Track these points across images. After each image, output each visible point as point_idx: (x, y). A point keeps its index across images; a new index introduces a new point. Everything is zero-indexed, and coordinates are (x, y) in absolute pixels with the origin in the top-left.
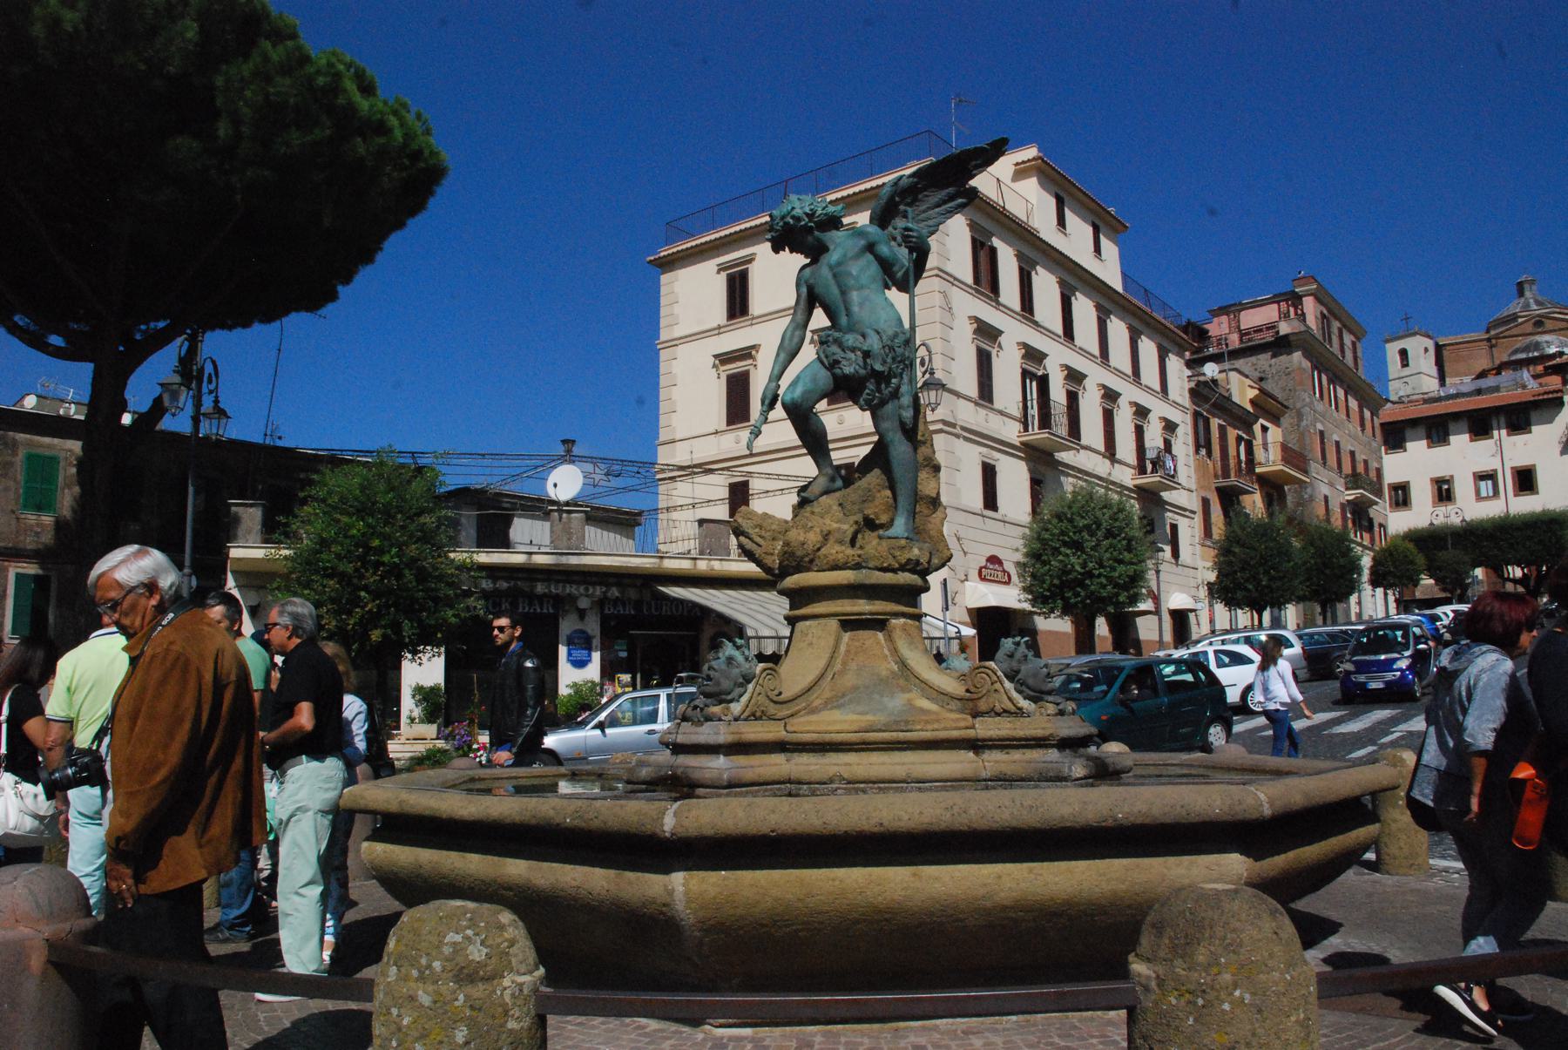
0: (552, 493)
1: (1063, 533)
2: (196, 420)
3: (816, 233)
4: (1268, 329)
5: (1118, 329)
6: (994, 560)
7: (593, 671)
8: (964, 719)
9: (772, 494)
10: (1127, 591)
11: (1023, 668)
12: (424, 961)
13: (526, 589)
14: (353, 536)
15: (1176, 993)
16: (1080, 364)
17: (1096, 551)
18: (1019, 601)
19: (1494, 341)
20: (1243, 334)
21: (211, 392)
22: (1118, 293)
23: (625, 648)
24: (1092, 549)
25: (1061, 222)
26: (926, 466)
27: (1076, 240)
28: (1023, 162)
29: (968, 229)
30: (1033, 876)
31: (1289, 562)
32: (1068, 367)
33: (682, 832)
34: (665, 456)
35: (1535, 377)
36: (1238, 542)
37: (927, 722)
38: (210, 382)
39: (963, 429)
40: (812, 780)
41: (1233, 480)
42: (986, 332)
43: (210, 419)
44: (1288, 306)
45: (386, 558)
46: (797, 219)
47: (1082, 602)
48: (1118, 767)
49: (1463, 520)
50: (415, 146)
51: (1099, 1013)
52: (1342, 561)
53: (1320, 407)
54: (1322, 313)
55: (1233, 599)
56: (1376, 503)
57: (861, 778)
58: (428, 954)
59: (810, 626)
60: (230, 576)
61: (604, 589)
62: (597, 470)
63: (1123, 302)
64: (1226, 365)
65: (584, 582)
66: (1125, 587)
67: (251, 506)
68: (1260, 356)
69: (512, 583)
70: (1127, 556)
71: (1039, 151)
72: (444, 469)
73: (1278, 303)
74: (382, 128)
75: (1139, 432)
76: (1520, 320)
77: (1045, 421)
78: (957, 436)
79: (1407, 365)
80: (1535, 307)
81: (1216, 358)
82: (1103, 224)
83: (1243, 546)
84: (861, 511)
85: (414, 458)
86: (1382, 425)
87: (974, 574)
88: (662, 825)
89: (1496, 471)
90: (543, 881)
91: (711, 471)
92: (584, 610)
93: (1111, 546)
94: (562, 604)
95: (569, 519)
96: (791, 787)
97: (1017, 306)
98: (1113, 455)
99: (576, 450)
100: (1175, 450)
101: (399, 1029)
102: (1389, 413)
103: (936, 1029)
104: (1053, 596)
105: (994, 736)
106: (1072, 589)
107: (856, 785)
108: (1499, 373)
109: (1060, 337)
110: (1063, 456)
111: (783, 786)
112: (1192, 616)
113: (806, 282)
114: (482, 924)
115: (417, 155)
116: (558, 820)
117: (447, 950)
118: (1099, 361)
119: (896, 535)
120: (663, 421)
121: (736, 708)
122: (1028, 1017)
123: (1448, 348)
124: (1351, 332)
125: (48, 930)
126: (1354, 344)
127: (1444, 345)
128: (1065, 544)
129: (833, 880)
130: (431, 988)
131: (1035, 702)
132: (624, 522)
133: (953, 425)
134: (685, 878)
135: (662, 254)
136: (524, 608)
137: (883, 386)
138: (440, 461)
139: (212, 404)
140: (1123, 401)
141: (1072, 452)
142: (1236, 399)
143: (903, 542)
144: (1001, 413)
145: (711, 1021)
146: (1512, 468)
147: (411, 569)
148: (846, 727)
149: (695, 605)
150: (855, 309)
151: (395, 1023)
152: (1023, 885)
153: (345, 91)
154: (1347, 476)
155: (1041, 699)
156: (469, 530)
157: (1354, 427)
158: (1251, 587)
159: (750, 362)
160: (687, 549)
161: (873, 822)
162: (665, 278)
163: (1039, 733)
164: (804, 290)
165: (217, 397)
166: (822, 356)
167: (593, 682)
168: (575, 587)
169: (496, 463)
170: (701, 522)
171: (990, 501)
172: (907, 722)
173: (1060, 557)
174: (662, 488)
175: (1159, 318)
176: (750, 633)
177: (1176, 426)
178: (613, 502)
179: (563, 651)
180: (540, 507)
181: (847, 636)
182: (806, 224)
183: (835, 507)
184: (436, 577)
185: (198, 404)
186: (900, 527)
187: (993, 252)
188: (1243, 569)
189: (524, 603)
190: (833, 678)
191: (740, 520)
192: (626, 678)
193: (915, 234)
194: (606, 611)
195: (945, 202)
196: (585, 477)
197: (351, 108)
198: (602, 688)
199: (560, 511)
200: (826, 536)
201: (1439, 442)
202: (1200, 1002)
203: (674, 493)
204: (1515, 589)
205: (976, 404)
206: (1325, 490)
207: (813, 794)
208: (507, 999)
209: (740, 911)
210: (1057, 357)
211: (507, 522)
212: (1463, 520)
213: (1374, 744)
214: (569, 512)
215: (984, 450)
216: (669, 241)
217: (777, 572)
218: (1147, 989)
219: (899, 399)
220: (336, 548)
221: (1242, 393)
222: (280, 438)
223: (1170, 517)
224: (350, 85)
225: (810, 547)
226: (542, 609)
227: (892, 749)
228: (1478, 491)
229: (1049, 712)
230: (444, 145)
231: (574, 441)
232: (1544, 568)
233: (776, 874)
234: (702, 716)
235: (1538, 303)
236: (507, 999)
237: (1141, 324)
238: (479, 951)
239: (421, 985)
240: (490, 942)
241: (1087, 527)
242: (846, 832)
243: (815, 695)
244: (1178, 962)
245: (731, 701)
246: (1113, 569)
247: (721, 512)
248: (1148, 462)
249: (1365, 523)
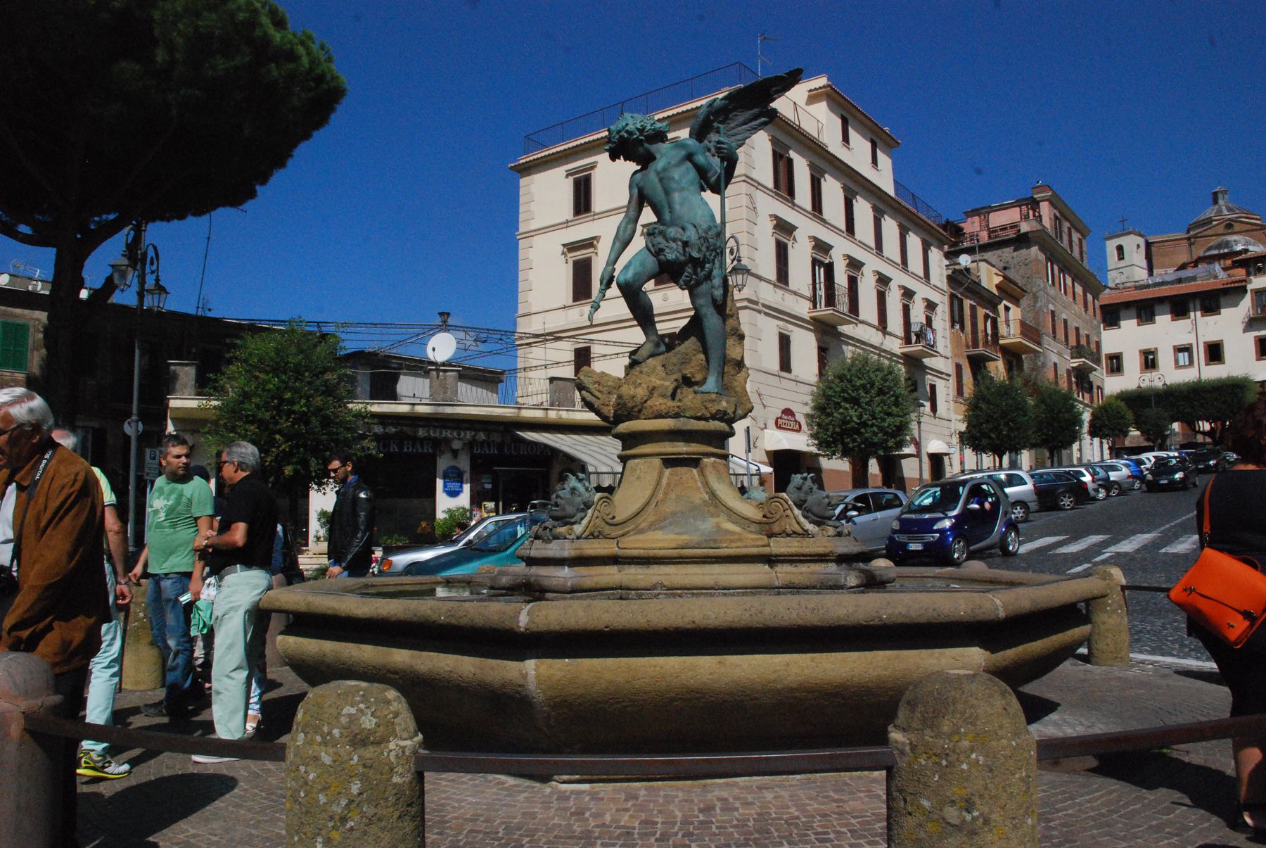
0: (431, 356)
1: (843, 391)
2: (141, 295)
3: (646, 145)
4: (1012, 227)
5: (890, 226)
6: (788, 412)
7: (464, 500)
8: (761, 539)
9: (609, 357)
10: (895, 438)
11: (809, 498)
12: (325, 729)
13: (410, 433)
14: (269, 390)
15: (925, 755)
16: (859, 254)
17: (870, 405)
18: (808, 445)
19: (1192, 240)
20: (991, 232)
21: (153, 272)
22: (889, 196)
23: (490, 481)
24: (866, 404)
25: (846, 138)
26: (733, 335)
27: (858, 153)
28: (816, 89)
29: (769, 143)
30: (814, 664)
31: (1025, 416)
32: (849, 257)
33: (534, 628)
34: (526, 326)
35: (1225, 269)
36: (984, 400)
37: (732, 541)
38: (152, 263)
39: (764, 306)
40: (639, 587)
41: (981, 349)
42: (784, 228)
43: (153, 294)
44: (1028, 209)
45: (296, 408)
46: (630, 133)
47: (858, 446)
48: (885, 578)
49: (1165, 384)
50: (318, 71)
51: (866, 773)
52: (1067, 416)
53: (1052, 291)
54: (1055, 214)
55: (979, 445)
56: (1095, 370)
57: (679, 586)
58: (328, 724)
59: (638, 463)
60: (169, 422)
61: (473, 433)
62: (468, 337)
63: (893, 203)
64: (977, 257)
65: (454, 428)
66: (893, 435)
67: (187, 365)
68: (1004, 250)
69: (399, 428)
71: (828, 80)
72: (343, 336)
73: (1020, 206)
74: (292, 56)
75: (906, 310)
76: (1214, 223)
77: (830, 301)
78: (760, 312)
79: (1123, 258)
80: (1227, 213)
81: (970, 251)
82: (879, 140)
83: (988, 402)
84: (680, 371)
85: (319, 326)
86: (1101, 307)
87: (771, 423)
88: (518, 622)
89: (1191, 345)
90: (422, 667)
91: (560, 339)
92: (458, 450)
93: (882, 401)
94: (440, 445)
95: (445, 379)
96: (622, 592)
97: (809, 207)
98: (885, 328)
99: (451, 321)
100: (934, 325)
101: (306, 783)
102: (1107, 297)
103: (736, 784)
104: (835, 441)
105: (786, 553)
107: (673, 591)
108: (1196, 266)
109: (843, 232)
110: (844, 329)
111: (615, 592)
112: (946, 459)
113: (637, 185)
114: (373, 700)
115: (320, 79)
116: (434, 617)
117: (344, 720)
118: (874, 252)
119: (708, 390)
120: (521, 297)
121: (578, 529)
122: (809, 776)
123: (1156, 245)
124: (1078, 231)
125: (24, 705)
126: (1080, 240)
127: (1154, 243)
128: (845, 400)
129: (655, 666)
130: (331, 750)
131: (818, 526)
132: (489, 379)
133: (756, 303)
134: (536, 664)
135: (521, 162)
136: (408, 449)
137: (699, 269)
138: (341, 329)
139: (154, 282)
140: (893, 285)
141: (851, 326)
142: (984, 284)
143: (714, 396)
144: (795, 293)
145: (556, 777)
146: (1205, 343)
147: (317, 417)
148: (666, 545)
149: (546, 446)
150: (677, 207)
151: (303, 778)
152: (806, 671)
153: (261, 25)
154: (1072, 348)
155: (824, 524)
156: (364, 385)
157: (1079, 308)
158: (994, 436)
159: (592, 250)
160: (540, 401)
161: (686, 620)
162: (523, 181)
163: (821, 550)
164: (636, 191)
165: (158, 276)
166: (650, 245)
167: (464, 508)
168: (449, 431)
169: (384, 331)
170: (552, 380)
171: (785, 365)
172: (715, 541)
173: (841, 410)
174: (520, 352)
175: (924, 218)
176: (591, 469)
177: (937, 305)
178: (480, 363)
179: (440, 483)
180: (421, 367)
181: (668, 472)
182: (637, 138)
183: (660, 368)
184: (337, 423)
185: (142, 282)
186: (711, 384)
187: (790, 162)
188: (988, 421)
189: (408, 443)
190: (656, 506)
191: (582, 378)
192: (491, 505)
193: (723, 146)
194: (475, 451)
195: (751, 120)
196: (458, 343)
197: (266, 40)
198: (471, 513)
199: (438, 370)
200: (652, 391)
201: (1147, 320)
202: (944, 763)
203: (530, 356)
204: (1204, 439)
205: (775, 285)
206: (1054, 358)
207: (640, 597)
208: (393, 759)
209: (580, 691)
210: (841, 249)
211: (394, 379)
212: (1165, 384)
213: (1089, 562)
214: (445, 371)
215: (781, 323)
216: (526, 152)
217: (612, 419)
218: (902, 753)
219: (711, 280)
220: (256, 400)
221: (990, 280)
222: (210, 310)
223: (929, 379)
224: (265, 20)
225: (638, 399)
226: (422, 448)
227: (705, 563)
228: (1176, 361)
229: (829, 534)
230: (342, 71)
231: (448, 314)
232: (1228, 423)
233: (610, 662)
234: (552, 535)
235: (1229, 209)
236: (393, 759)
237: (909, 222)
238: (370, 721)
239: (324, 748)
240: (378, 714)
241: (863, 386)
242: (665, 628)
243: (642, 519)
244: (928, 731)
245: (574, 523)
246: (883, 420)
247: (568, 372)
248: (913, 335)
249: (1086, 385)
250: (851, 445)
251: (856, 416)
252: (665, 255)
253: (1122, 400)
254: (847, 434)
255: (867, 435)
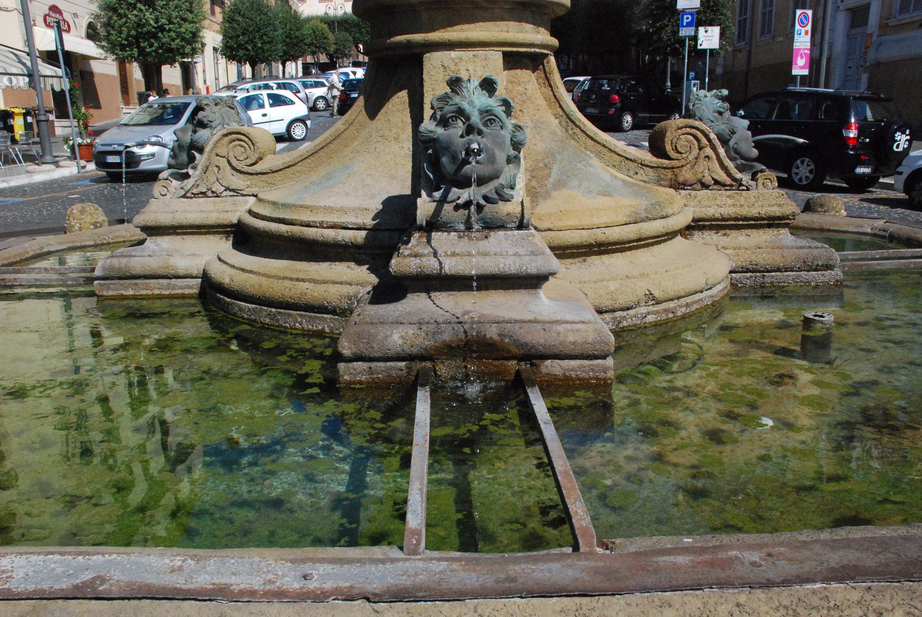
10: (190, 45)
17: (166, 9)
36: (239, 13)
47: (156, 51)
66: (189, 42)
70: (190, 16)
83: (243, 16)
104: (130, 45)
106: (147, 40)
173: (135, 12)
188: (244, 34)
250: (148, 50)
251: (153, 20)
253: (325, 23)
254: (142, 38)
255: (164, 40)
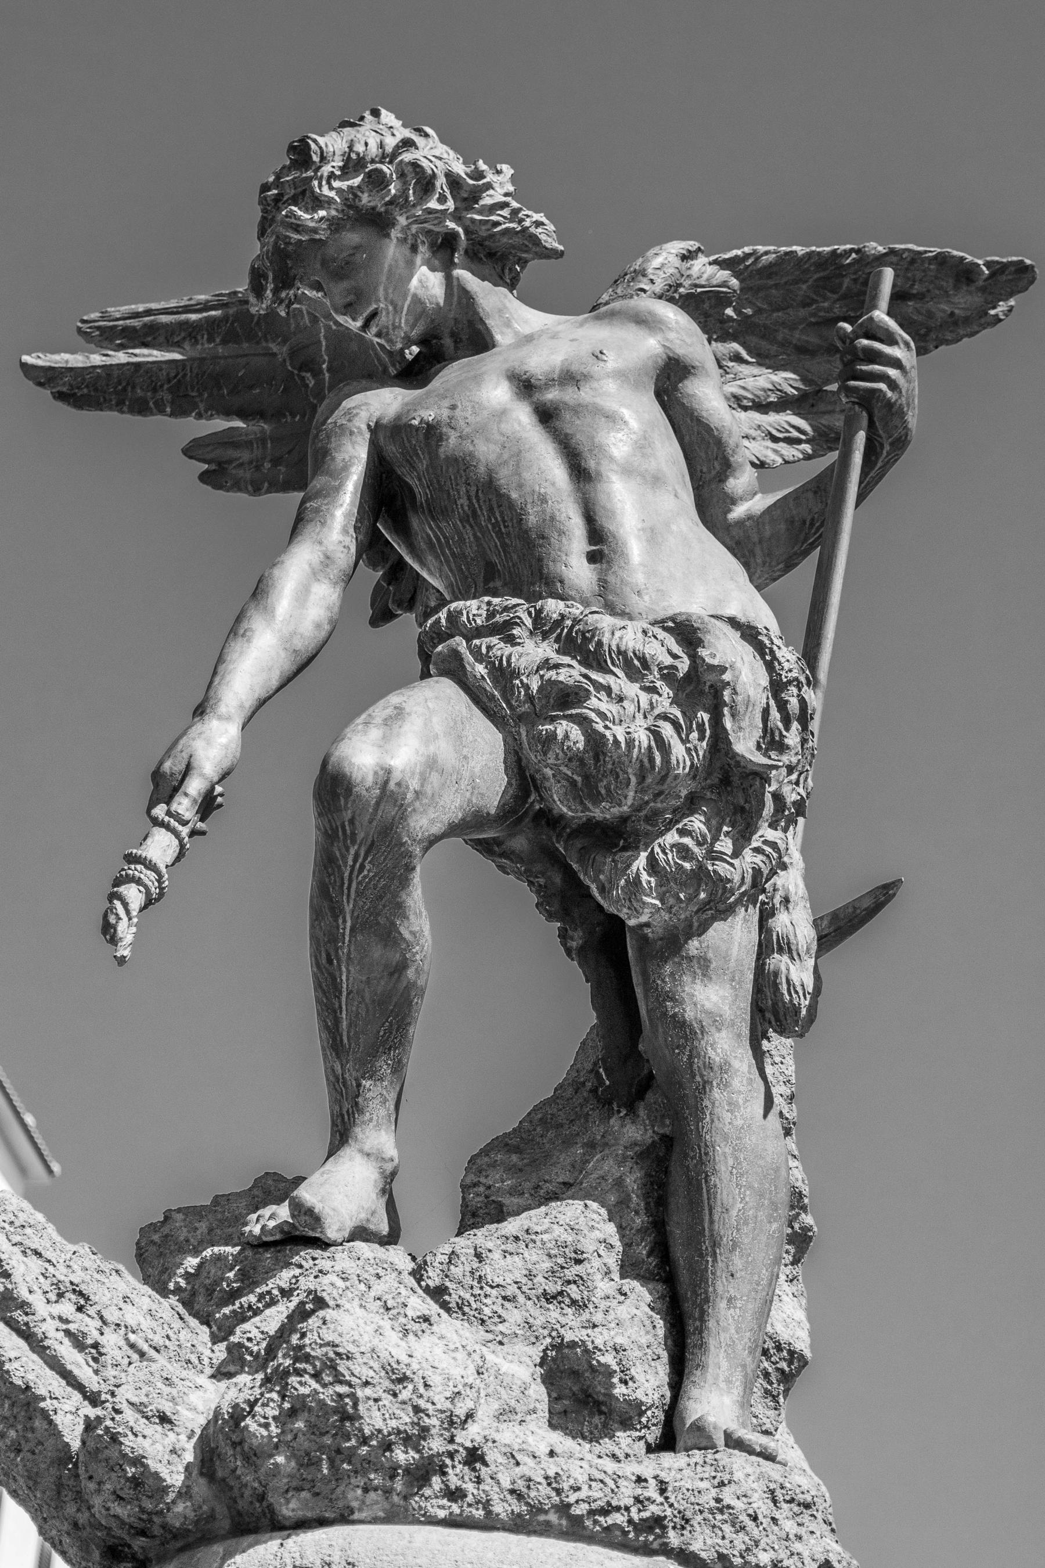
219: (766, 915)
252: (582, 721)
